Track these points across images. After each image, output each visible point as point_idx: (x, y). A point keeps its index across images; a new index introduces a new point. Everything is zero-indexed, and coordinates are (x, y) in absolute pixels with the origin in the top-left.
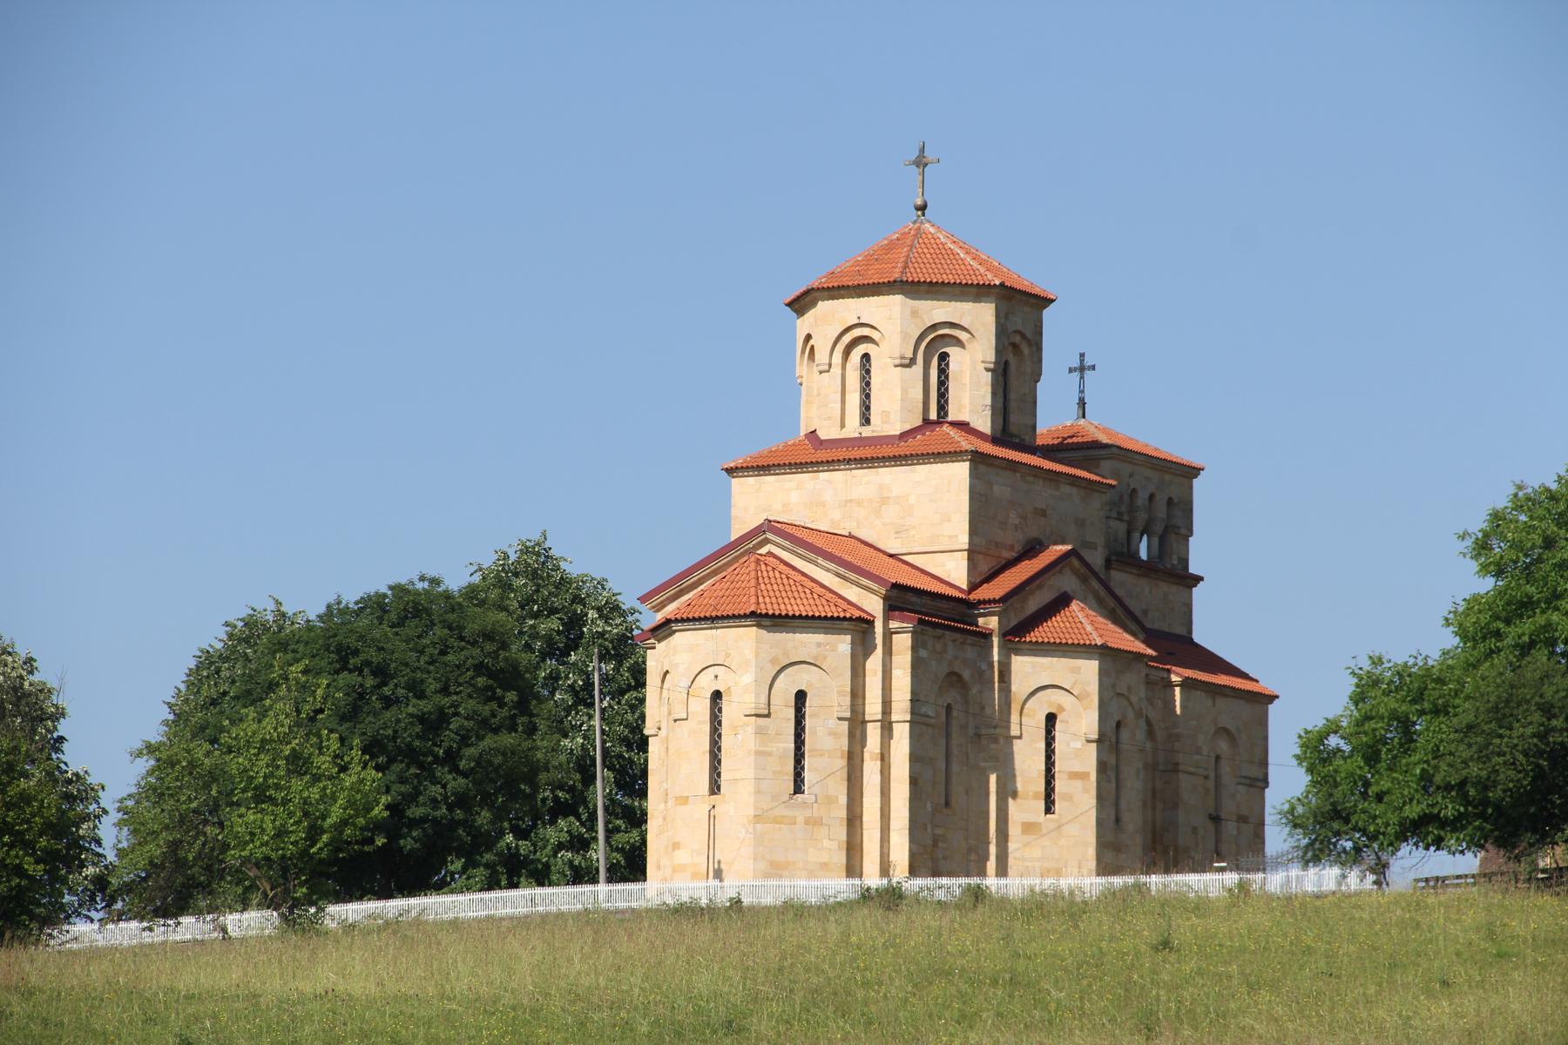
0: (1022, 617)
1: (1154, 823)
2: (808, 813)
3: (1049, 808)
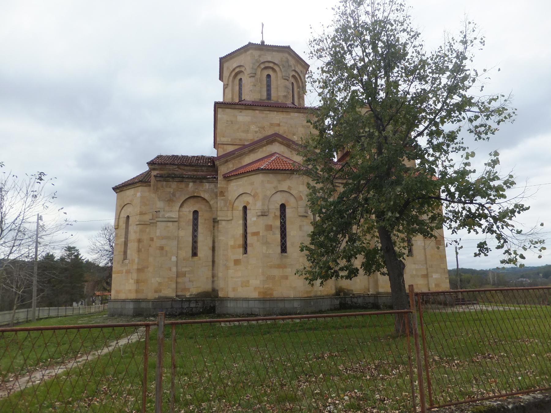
0: (240, 166)
3: (245, 252)
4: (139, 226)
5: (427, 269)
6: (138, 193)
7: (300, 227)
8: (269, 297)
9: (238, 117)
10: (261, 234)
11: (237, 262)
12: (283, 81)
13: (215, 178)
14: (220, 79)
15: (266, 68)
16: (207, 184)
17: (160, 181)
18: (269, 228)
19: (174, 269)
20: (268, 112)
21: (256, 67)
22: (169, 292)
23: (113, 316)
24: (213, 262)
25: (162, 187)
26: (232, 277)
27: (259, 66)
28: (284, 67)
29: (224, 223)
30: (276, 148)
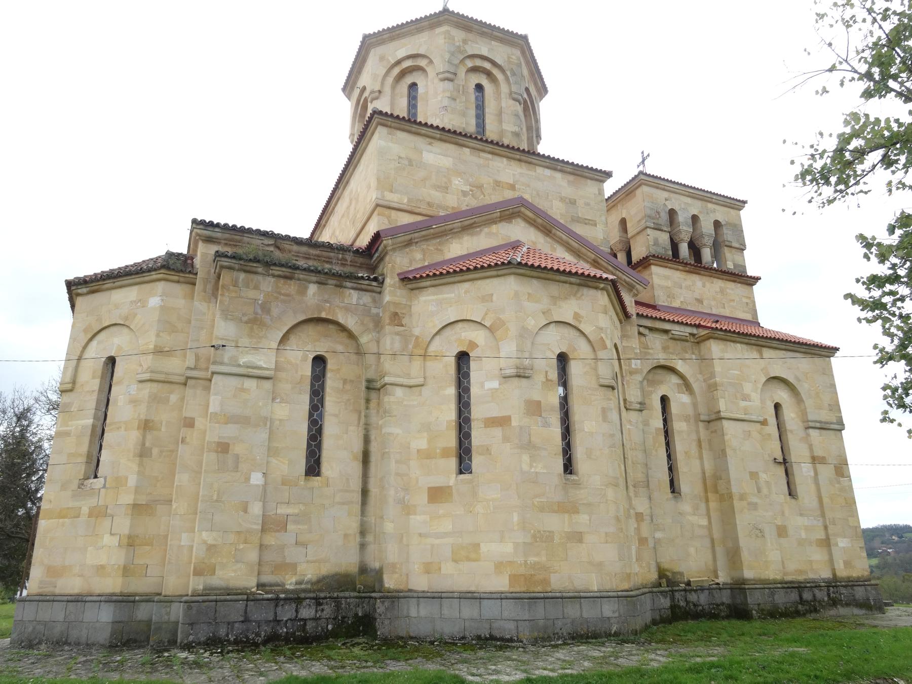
0: (439, 258)
1: (704, 473)
2: (93, 502)
4: (149, 384)
5: (826, 528)
6: (156, 297)
7: (604, 411)
8: (539, 589)
9: (425, 154)
10: (514, 423)
11: (437, 494)
12: (511, 102)
13: (375, 279)
14: (344, 90)
15: (475, 69)
16: (355, 294)
17: (230, 268)
18: (534, 408)
19: (256, 509)
20: (490, 156)
21: (456, 62)
22: (237, 574)
23: (31, 646)
24: (365, 492)
25: (235, 285)
26: (420, 535)
27: (462, 61)
28: (514, 74)
29: (399, 392)
30: (518, 231)
